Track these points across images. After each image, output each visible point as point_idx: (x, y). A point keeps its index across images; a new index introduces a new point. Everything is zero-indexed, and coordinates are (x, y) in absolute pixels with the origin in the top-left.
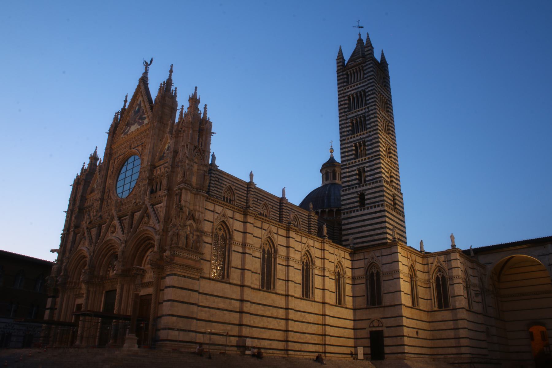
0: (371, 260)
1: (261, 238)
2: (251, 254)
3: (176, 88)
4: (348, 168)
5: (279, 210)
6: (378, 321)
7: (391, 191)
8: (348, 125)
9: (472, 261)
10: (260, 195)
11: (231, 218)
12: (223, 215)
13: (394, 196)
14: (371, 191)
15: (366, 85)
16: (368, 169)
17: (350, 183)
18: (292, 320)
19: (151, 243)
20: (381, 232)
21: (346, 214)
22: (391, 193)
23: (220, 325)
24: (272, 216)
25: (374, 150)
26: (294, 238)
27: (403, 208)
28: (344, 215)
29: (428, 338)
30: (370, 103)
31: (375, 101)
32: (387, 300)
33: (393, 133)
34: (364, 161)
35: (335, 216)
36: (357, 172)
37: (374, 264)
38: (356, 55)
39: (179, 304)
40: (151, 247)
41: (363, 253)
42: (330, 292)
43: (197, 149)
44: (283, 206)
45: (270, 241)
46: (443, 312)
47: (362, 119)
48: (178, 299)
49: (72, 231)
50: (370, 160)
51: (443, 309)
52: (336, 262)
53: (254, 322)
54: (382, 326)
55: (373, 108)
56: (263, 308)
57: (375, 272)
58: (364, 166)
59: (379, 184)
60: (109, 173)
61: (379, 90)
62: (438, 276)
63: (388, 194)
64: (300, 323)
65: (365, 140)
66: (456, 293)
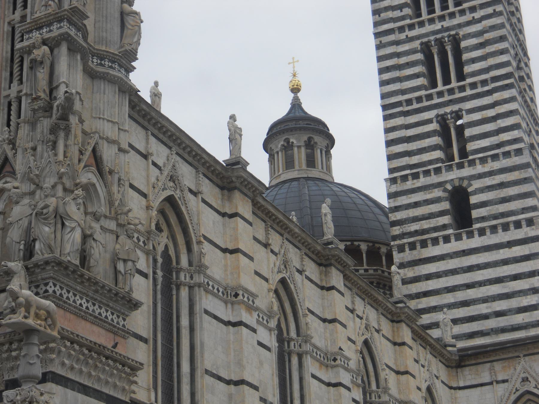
0: (518, 385)
11: (191, 191)
12: (172, 178)
14: (488, 181)
16: (476, 116)
17: (415, 160)
21: (407, 249)
25: (492, 61)
28: (402, 254)
34: (458, 95)
36: (434, 126)
41: (488, 365)
50: (480, 90)
52: (424, 387)
58: (461, 110)
65: (457, 34)
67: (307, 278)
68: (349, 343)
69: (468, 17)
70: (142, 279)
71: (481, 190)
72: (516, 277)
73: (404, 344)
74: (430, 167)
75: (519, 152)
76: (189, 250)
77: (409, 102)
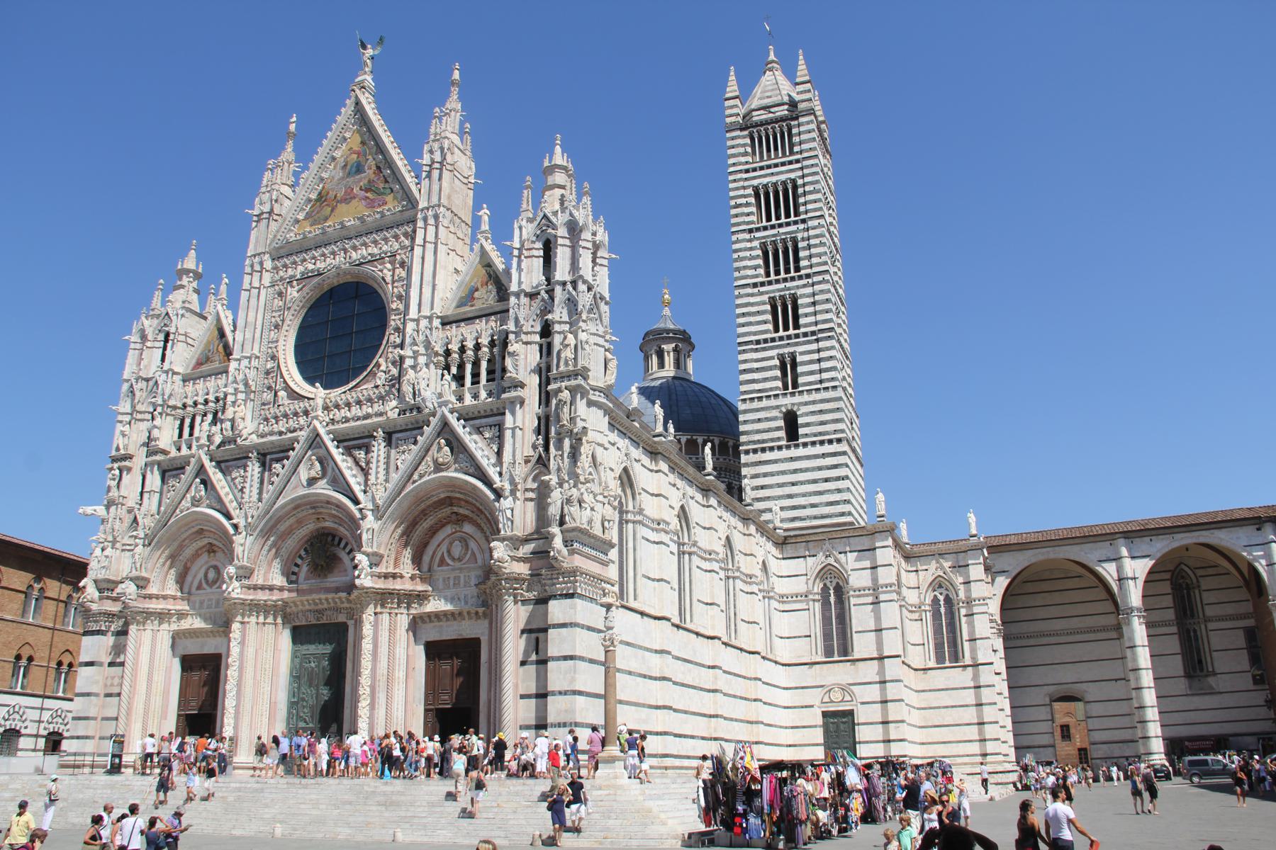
4: (756, 350)
8: (754, 253)
23: (633, 708)
25: (819, 317)
31: (820, 209)
32: (863, 645)
36: (776, 362)
37: (829, 567)
38: (768, 97)
40: (448, 523)
45: (683, 514)
47: (790, 244)
51: (947, 664)
58: (795, 352)
59: (831, 394)
62: (935, 596)
66: (977, 632)
69: (804, 282)
71: (807, 414)
72: (826, 480)
75: (835, 388)
77: (758, 342)
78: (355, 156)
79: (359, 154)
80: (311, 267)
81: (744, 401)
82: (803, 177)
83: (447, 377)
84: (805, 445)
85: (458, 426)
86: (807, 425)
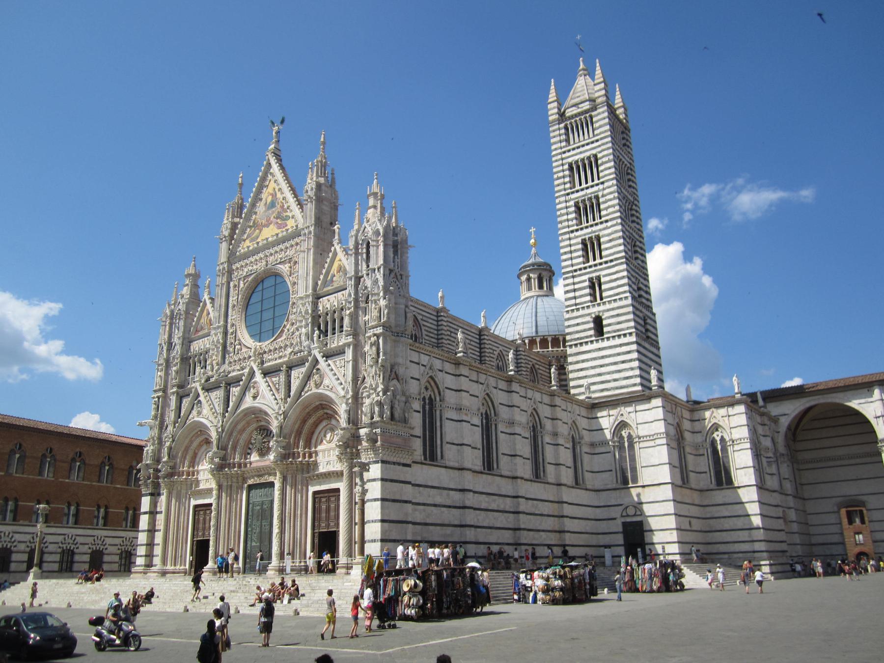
1: (477, 397)
2: (469, 422)
3: (333, 170)
4: (573, 277)
5: (478, 346)
6: (635, 507)
7: (641, 312)
9: (762, 415)
10: (454, 326)
11: (440, 371)
12: (430, 368)
13: (645, 320)
15: (599, 146)
17: (578, 301)
18: (524, 513)
19: (327, 413)
20: (631, 375)
22: (641, 315)
23: (438, 528)
24: (471, 355)
26: (518, 393)
27: (657, 336)
29: (704, 529)
30: (606, 176)
33: (639, 221)
35: (550, 349)
36: (587, 284)
38: (579, 97)
39: (390, 503)
40: (324, 419)
42: (567, 467)
43: (392, 275)
44: (484, 339)
46: (723, 491)
47: (594, 201)
48: (388, 497)
49: (173, 393)
52: (570, 422)
53: (478, 520)
54: (641, 515)
55: (610, 183)
56: (487, 499)
57: (624, 433)
60: (231, 299)
61: (618, 154)
63: (638, 316)
64: (532, 517)
67: (500, 389)
68: (523, 412)
69: (604, 225)
70: (418, 414)
71: (609, 318)
72: (623, 362)
73: (555, 406)
74: (585, 305)
75: (626, 298)
76: (440, 394)
77: (576, 271)
78: (270, 197)
79: (272, 195)
80: (250, 268)
81: (568, 312)
82: (600, 152)
83: (317, 332)
84: (608, 338)
85: (321, 360)
86: (609, 325)
